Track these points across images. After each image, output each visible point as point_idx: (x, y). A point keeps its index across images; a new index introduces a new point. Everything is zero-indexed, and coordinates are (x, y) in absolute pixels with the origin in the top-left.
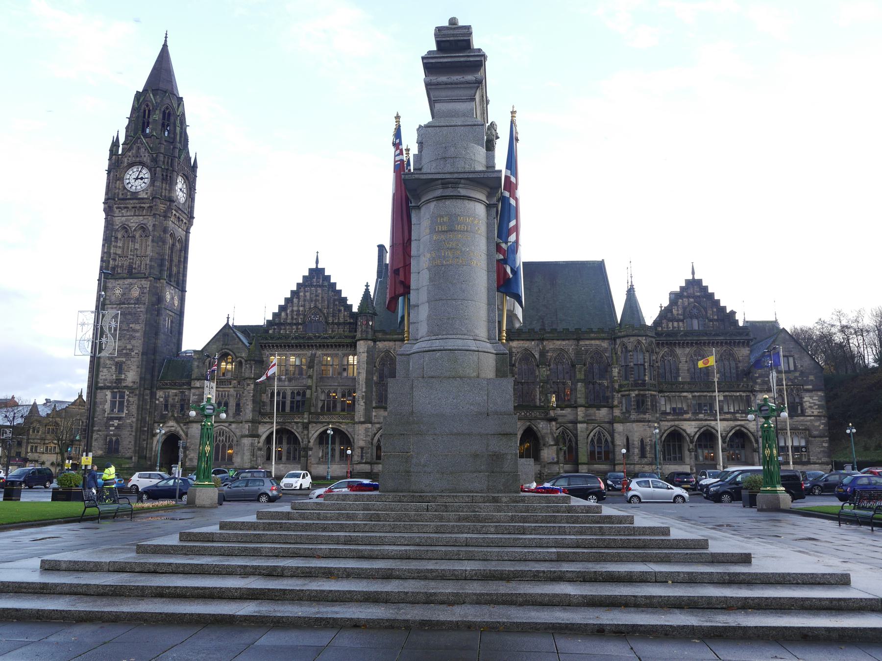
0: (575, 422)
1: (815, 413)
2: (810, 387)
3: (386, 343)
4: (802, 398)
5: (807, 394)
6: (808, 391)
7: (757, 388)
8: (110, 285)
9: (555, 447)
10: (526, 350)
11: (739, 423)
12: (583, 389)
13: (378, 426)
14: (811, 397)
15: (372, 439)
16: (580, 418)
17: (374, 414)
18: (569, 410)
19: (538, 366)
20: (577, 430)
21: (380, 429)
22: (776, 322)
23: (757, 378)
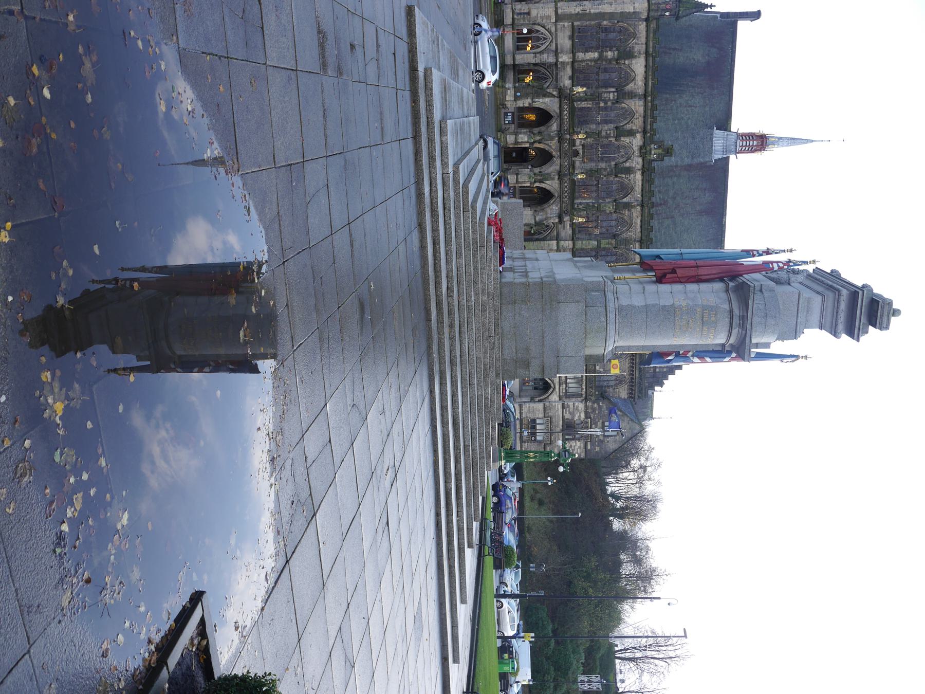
0: (558, 239)
3: (644, 33)
4: (579, 439)
5: (582, 445)
7: (589, 404)
9: (533, 222)
10: (632, 189)
11: (557, 387)
12: (590, 246)
13: (553, 29)
14: (580, 447)
15: (538, 24)
16: (562, 243)
17: (566, 24)
18: (570, 232)
19: (615, 201)
20: (551, 240)
21: (550, 32)
22: (652, 418)
23: (598, 404)
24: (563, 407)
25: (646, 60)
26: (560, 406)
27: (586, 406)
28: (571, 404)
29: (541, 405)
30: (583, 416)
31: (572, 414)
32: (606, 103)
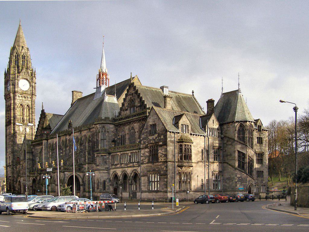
1: (163, 161)
2: (161, 143)
6: (161, 146)
8: (7, 129)
11: (135, 168)
14: (161, 150)
24: (143, 163)
25: (54, 138)
26: (142, 166)
27: (143, 149)
29: (142, 178)
30: (147, 150)
31: (146, 157)
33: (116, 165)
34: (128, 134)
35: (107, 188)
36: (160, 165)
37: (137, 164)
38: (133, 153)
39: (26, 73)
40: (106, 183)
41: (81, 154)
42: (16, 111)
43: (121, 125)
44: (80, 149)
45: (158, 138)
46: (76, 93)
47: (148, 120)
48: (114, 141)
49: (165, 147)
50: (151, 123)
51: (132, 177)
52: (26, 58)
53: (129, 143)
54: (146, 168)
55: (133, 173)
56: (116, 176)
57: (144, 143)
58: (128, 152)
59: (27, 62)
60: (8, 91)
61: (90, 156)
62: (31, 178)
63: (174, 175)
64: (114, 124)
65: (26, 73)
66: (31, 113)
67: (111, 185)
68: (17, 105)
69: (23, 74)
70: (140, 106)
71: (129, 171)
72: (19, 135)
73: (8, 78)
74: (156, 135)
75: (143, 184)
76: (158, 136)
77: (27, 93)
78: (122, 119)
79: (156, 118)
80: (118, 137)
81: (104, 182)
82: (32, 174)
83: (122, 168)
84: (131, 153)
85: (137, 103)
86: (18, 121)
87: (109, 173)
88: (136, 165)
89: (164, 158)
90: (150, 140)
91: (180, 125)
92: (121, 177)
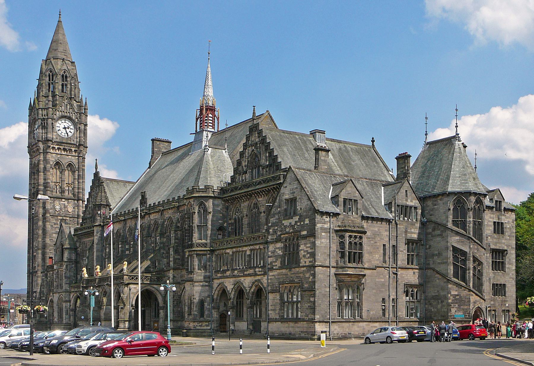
1: (307, 264)
2: (305, 233)
6: (305, 237)
14: (305, 244)
24: (271, 269)
26: (271, 274)
27: (272, 243)
28: (270, 260)
29: (271, 296)
30: (279, 245)
32: (127, 250)
33: (224, 271)
34: (247, 216)
35: (206, 313)
36: (303, 272)
37: (261, 269)
38: (254, 250)
39: (68, 107)
40: (206, 304)
41: (162, 251)
42: (49, 173)
43: (234, 199)
44: (161, 243)
45: (299, 224)
46: (158, 143)
47: (283, 190)
48: (221, 229)
49: (312, 239)
50: (287, 197)
51: (253, 293)
52: (69, 79)
53: (249, 233)
54: (277, 277)
55: (254, 287)
56: (224, 292)
57: (275, 232)
58: (245, 249)
59: (71, 87)
60: (34, 137)
61: (179, 255)
62: (71, 296)
63: (328, 290)
64: (222, 198)
65: (68, 107)
66: (77, 177)
67: (214, 308)
68: (51, 163)
69: (63, 108)
70: (270, 166)
71: (247, 282)
72: (53, 216)
73: (35, 114)
74: (296, 218)
75: (271, 305)
76: (300, 220)
77: (69, 142)
78: (236, 188)
79: (296, 188)
80: (230, 222)
81: (202, 303)
82: (74, 287)
83: (234, 276)
84: (251, 250)
85: (264, 161)
86: (52, 191)
87: (210, 286)
88: (259, 271)
89: (309, 260)
90: (286, 227)
91: (341, 200)
92: (233, 293)
